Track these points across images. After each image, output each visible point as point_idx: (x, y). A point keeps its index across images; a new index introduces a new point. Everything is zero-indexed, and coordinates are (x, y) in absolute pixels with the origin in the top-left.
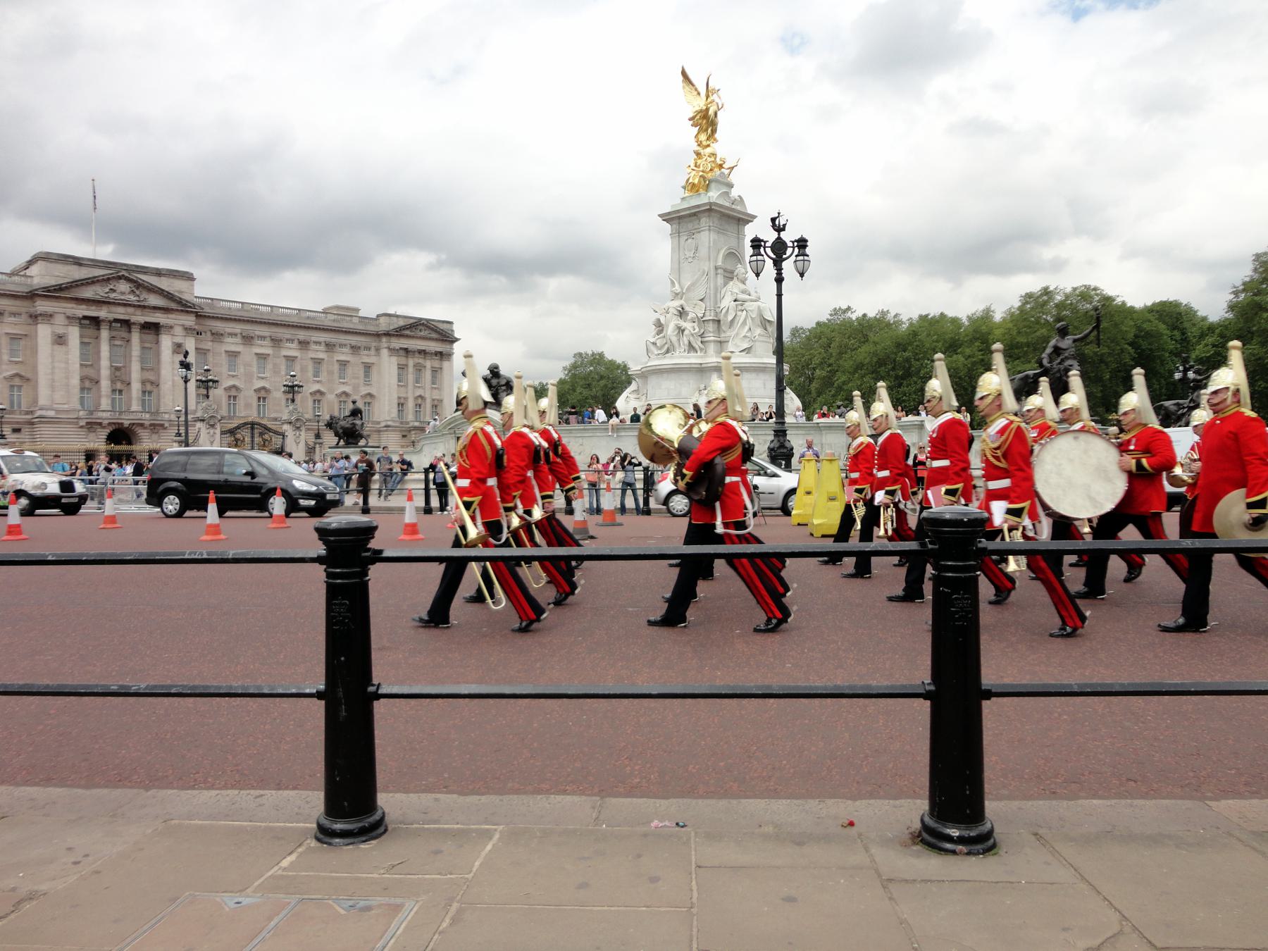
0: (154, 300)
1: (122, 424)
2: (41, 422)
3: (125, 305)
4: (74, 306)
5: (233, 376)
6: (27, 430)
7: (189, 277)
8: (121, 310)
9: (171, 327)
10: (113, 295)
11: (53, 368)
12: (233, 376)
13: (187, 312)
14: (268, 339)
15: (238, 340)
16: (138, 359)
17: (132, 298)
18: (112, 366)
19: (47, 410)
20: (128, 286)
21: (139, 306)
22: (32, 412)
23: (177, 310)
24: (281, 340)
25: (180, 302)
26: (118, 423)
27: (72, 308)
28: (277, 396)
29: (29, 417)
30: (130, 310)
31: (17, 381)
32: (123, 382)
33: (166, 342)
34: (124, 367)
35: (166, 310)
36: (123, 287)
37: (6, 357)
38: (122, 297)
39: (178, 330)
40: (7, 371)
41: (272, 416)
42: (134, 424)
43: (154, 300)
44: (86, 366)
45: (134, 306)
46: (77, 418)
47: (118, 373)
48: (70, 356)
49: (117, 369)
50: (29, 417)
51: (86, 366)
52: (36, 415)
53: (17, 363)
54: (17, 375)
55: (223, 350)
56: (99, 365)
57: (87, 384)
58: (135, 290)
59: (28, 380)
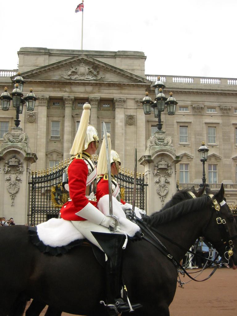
0: (110, 78)
3: (84, 84)
4: (43, 89)
5: (184, 146)
7: (140, 57)
8: (81, 89)
9: (124, 101)
10: (73, 77)
13: (138, 86)
14: (217, 109)
15: (189, 111)
17: (90, 78)
20: (87, 68)
21: (96, 84)
23: (129, 85)
24: (229, 109)
25: (131, 77)
27: (42, 91)
28: (228, 163)
30: (89, 89)
33: (120, 115)
35: (119, 86)
36: (83, 69)
38: (82, 78)
39: (131, 104)
43: (110, 78)
45: (92, 85)
48: (38, 132)
55: (175, 121)
57: (55, 156)
58: (93, 71)
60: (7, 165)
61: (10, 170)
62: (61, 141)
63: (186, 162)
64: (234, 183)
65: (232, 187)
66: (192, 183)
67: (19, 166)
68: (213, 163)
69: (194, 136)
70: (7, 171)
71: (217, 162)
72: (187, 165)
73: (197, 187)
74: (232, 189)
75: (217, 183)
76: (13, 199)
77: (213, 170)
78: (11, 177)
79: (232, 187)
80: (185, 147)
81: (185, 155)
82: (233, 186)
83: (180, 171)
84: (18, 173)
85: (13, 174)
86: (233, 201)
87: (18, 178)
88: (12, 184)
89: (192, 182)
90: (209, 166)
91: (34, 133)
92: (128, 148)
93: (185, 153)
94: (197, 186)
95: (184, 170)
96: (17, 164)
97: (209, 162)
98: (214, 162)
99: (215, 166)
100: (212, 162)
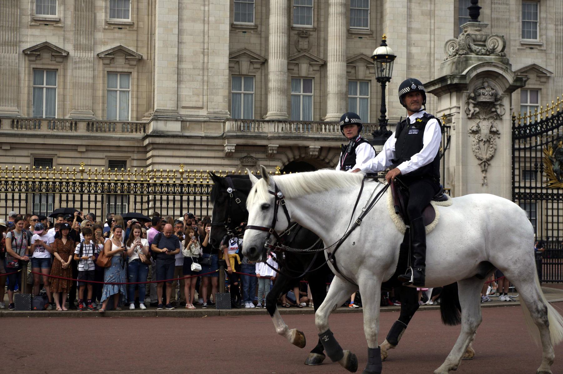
1: (307, 148)
2: (155, 146)
6: (135, 163)
11: (180, 32)
12: (531, 47)
16: (340, 9)
18: (290, 28)
19: (167, 119)
22: (144, 126)
26: (299, 148)
29: (140, 135)
31: (120, 64)
32: (312, 61)
34: (315, 29)
37: (102, 16)
40: (104, 43)
42: (330, 149)
44: (245, 30)
46: (222, 137)
47: (304, 44)
49: (304, 34)
50: (140, 135)
51: (245, 30)
52: (150, 131)
53: (121, 27)
54: (120, 50)
56: (268, 25)
57: (245, 66)
59: (140, 60)
62: (259, 29)
63: (534, 84)
69: (551, 26)
78: (480, 125)
80: (532, 51)
81: (534, 68)
88: (482, 140)
91: (202, 8)
92: (414, 50)
93: (534, 65)
95: (529, 104)
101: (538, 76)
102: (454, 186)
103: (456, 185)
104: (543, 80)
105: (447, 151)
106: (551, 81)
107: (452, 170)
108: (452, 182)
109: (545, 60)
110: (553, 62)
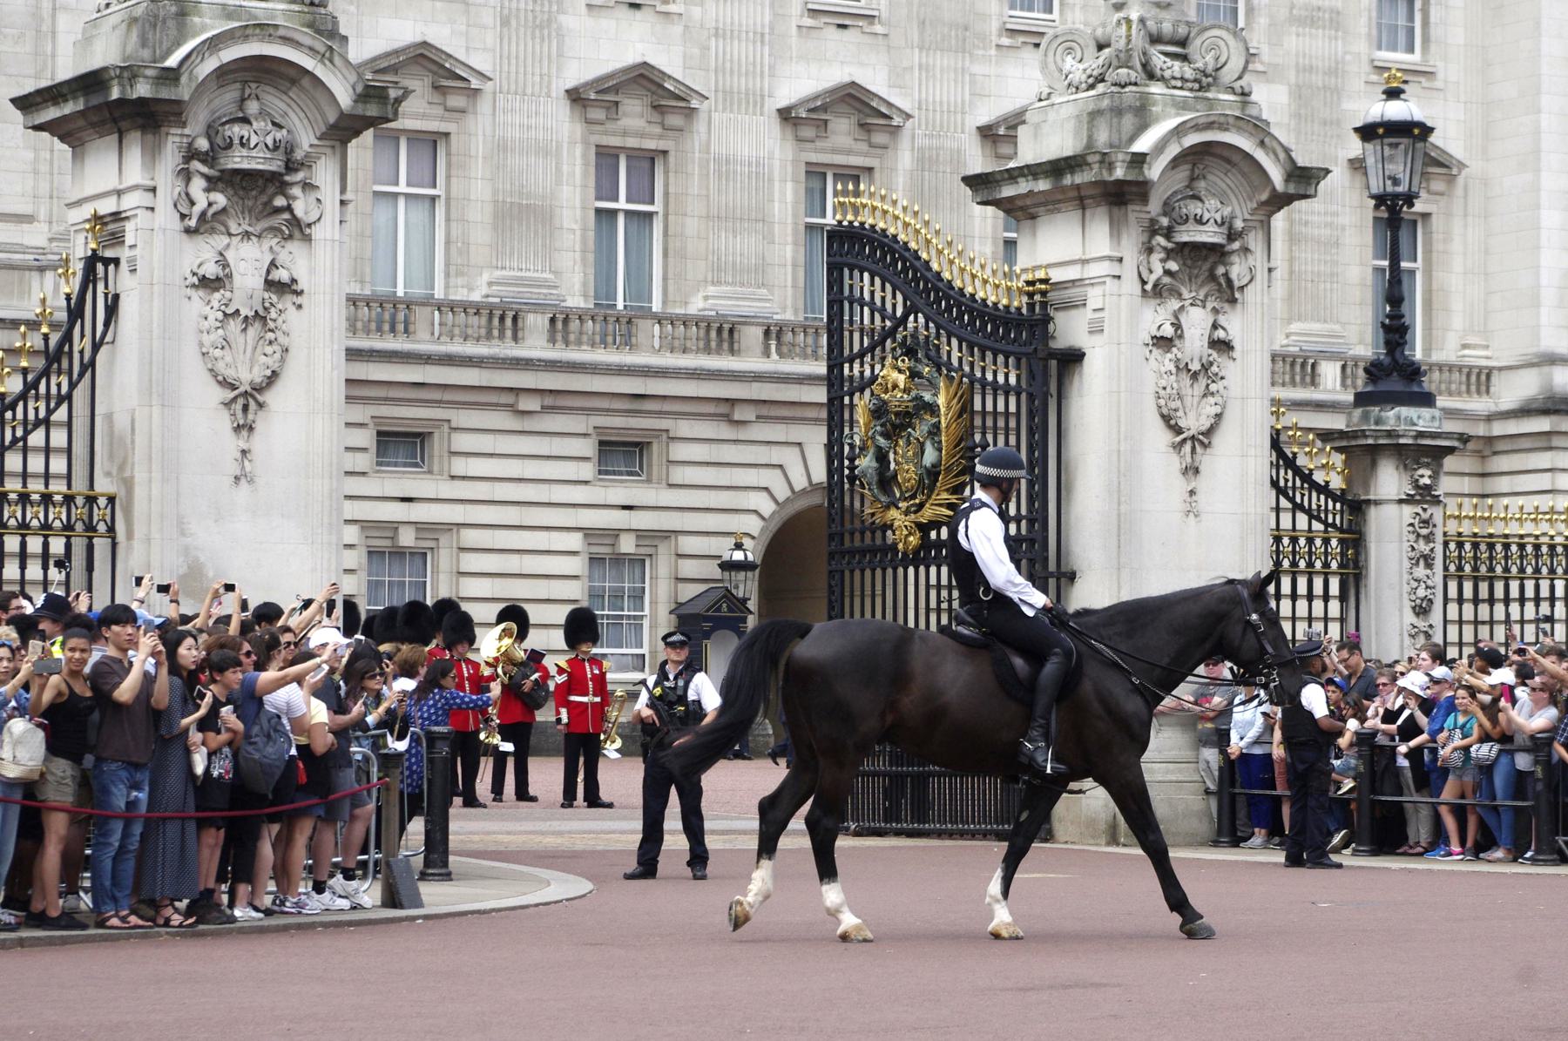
41: (696, 306)
60: (205, 169)
61: (224, 210)
63: (424, 116)
64: (586, 301)
65: (773, 343)
66: (460, 295)
67: (287, 178)
68: (632, 142)
70: (203, 214)
71: (661, 137)
72: (430, 143)
73: (509, 333)
74: (775, 364)
75: (620, 305)
76: (244, 428)
77: (629, 200)
78: (230, 256)
79: (773, 348)
81: (423, 57)
82: (788, 337)
83: (376, 193)
84: (275, 230)
85: (247, 235)
86: (776, 455)
87: (281, 275)
89: (471, 289)
90: (598, 166)
93: (425, 44)
94: (509, 322)
95: (402, 188)
96: (275, 166)
97: (606, 133)
98: (642, 135)
99: (647, 162)
100: (625, 134)
101: (436, 87)
102: (128, 484)
103: (137, 480)
104: (455, 101)
105: (103, 350)
106: (484, 105)
107: (122, 422)
108: (121, 468)
109: (463, 28)
110: (490, 39)
